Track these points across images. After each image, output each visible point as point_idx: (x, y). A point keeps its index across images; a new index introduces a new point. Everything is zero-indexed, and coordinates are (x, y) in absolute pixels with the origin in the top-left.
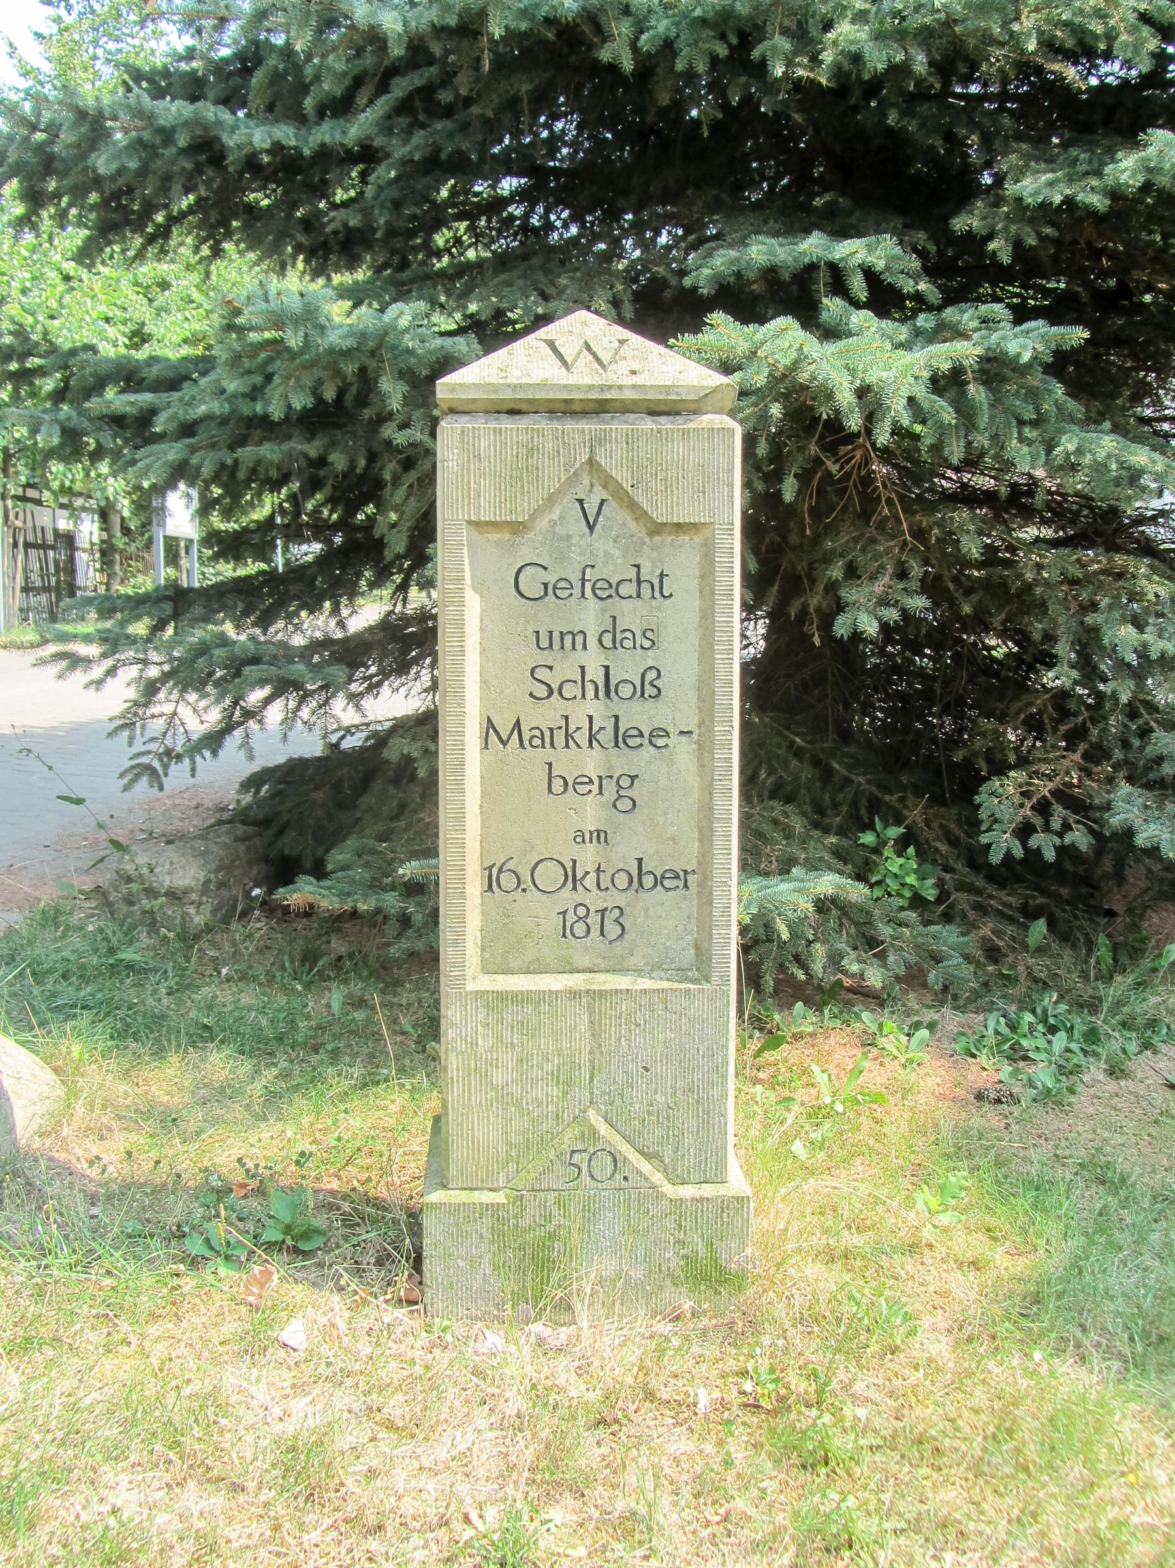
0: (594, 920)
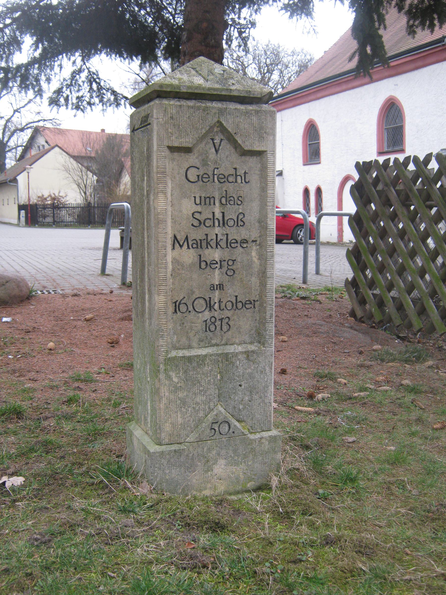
0: (218, 323)
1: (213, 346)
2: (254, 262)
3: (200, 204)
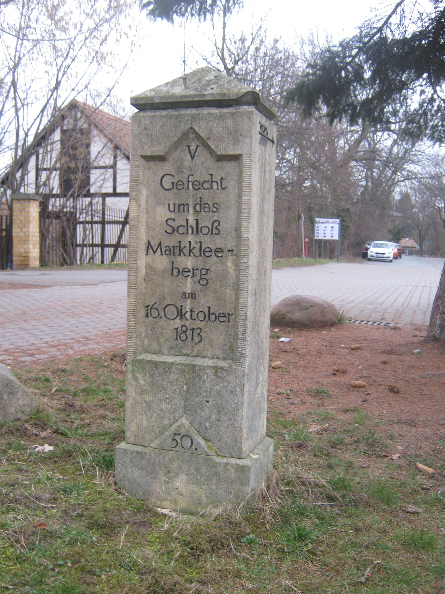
0: (189, 333)
1: (184, 355)
2: (230, 273)
3: (174, 211)
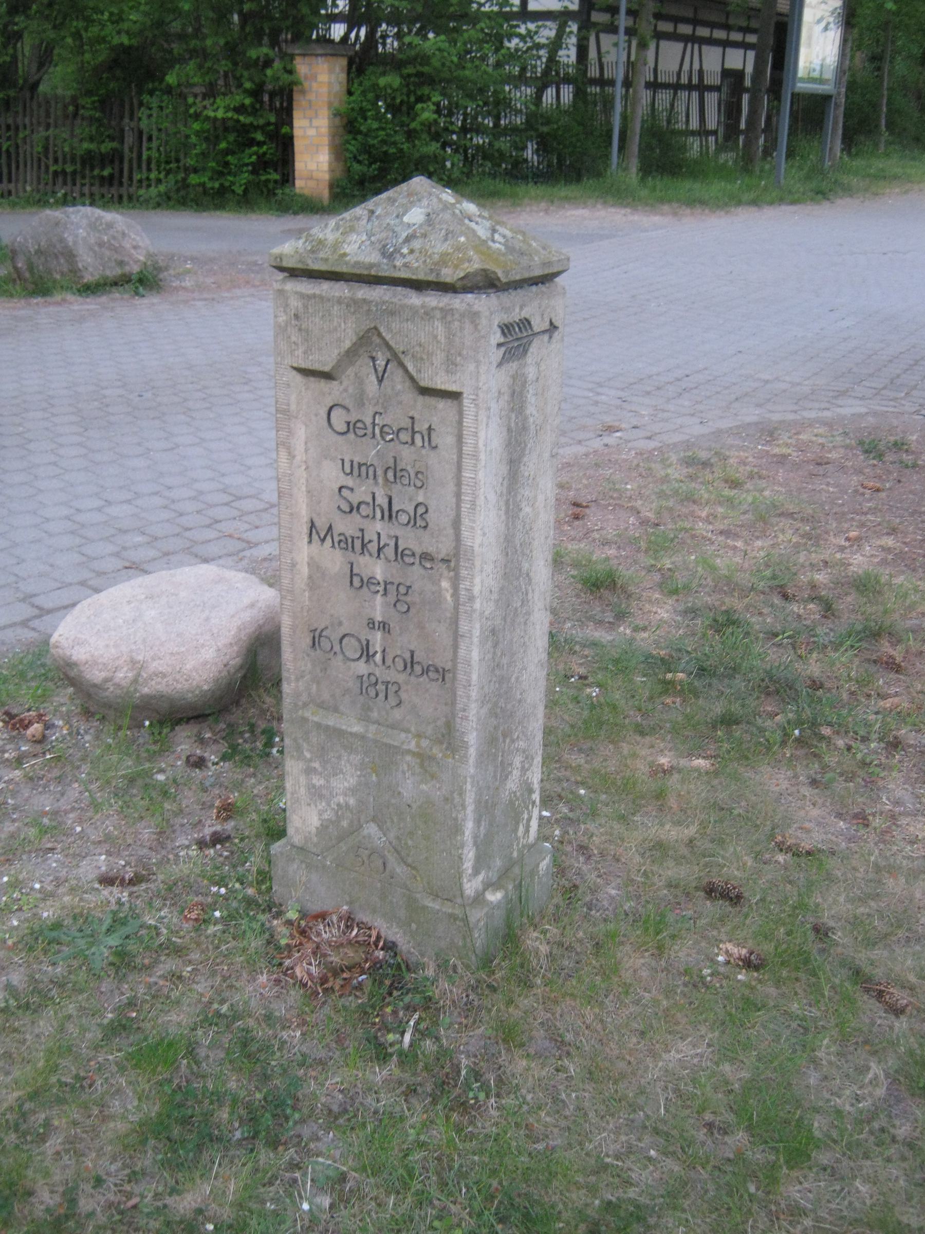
0: (381, 687)
3: (351, 473)
